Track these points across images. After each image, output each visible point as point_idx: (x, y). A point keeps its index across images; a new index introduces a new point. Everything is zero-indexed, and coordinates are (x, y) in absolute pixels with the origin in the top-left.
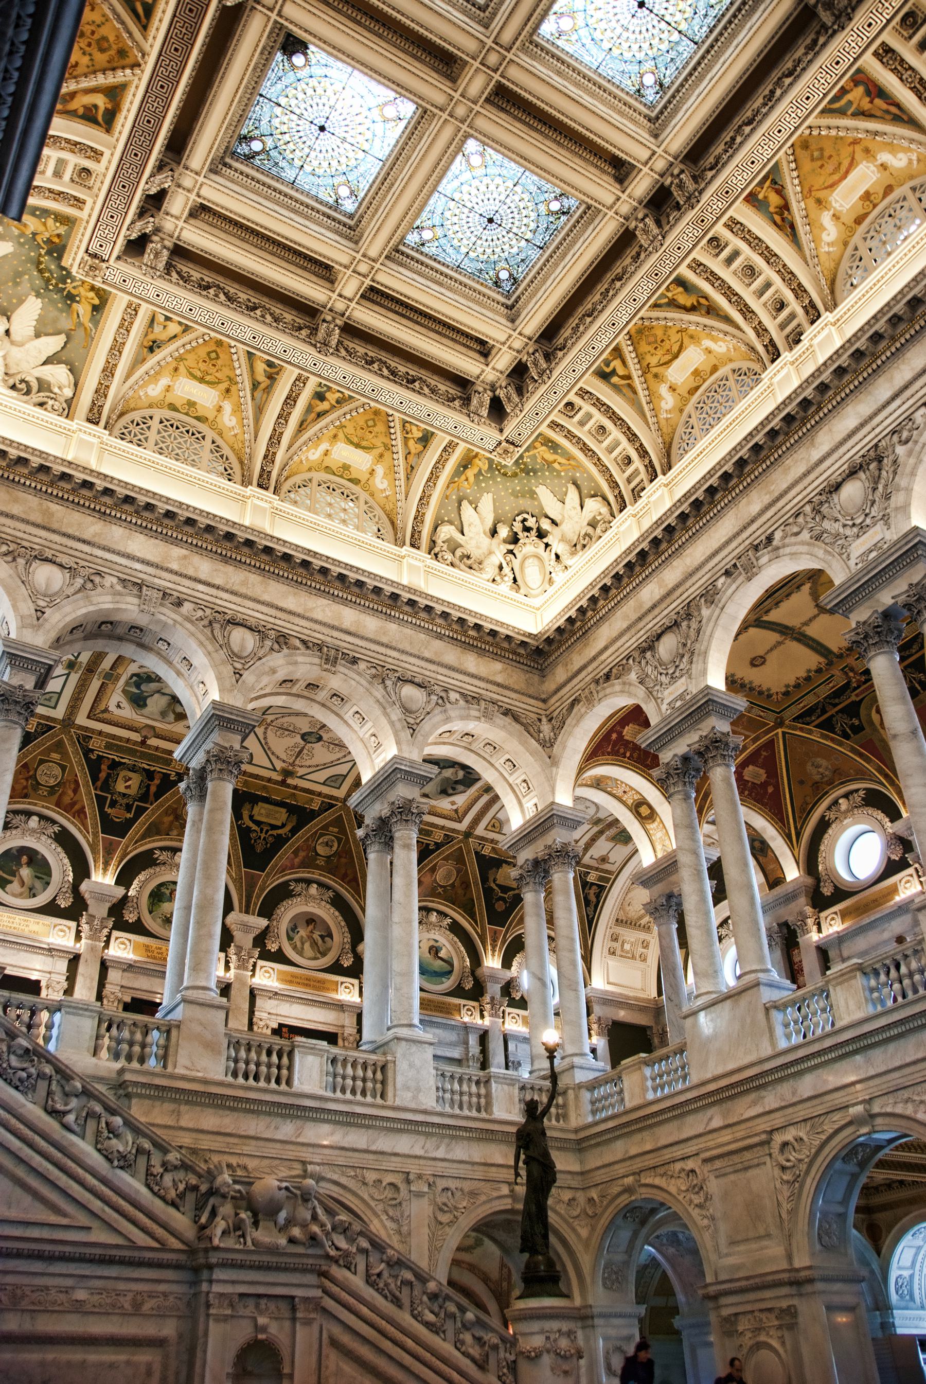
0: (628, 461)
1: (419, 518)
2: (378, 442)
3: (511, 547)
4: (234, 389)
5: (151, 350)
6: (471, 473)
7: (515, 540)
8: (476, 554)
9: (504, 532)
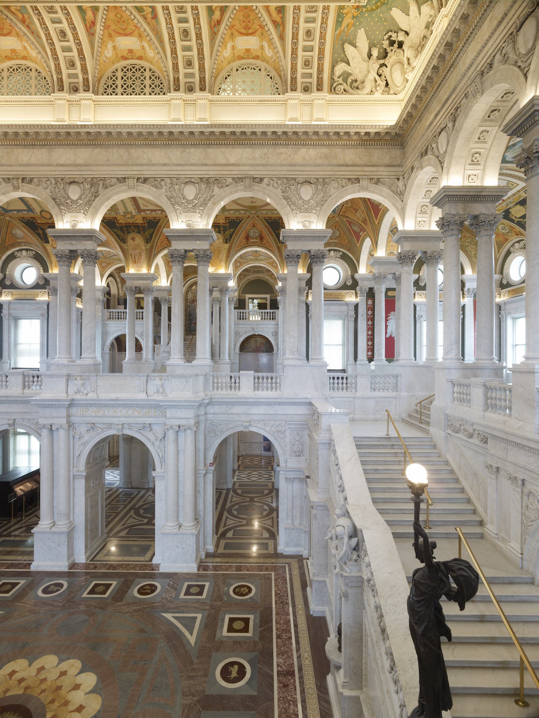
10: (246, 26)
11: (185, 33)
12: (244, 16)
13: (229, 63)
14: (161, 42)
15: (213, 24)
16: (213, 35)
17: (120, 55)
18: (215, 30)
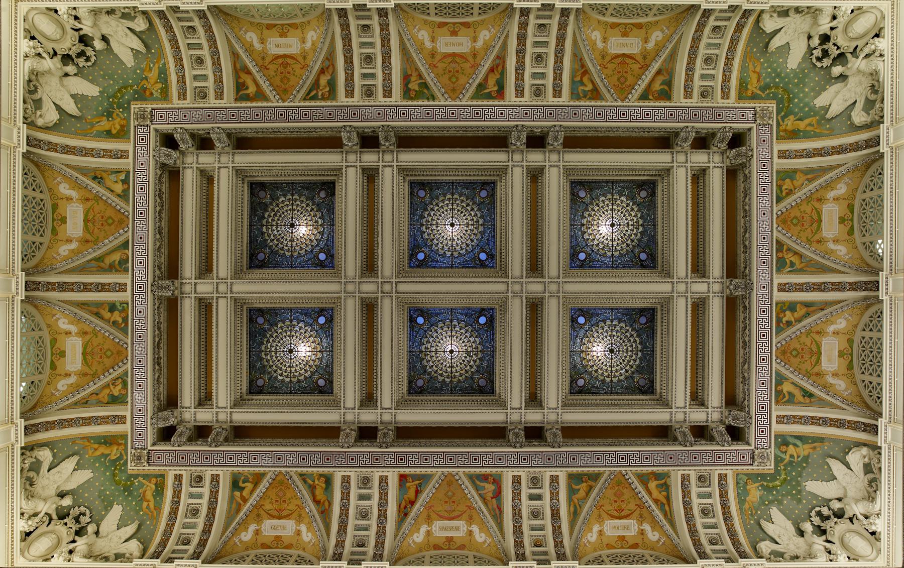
0: (716, 29)
1: (855, 147)
2: (808, 209)
3: (849, 56)
4: (814, 330)
5: (811, 395)
6: (802, 125)
7: (841, 58)
8: (867, 82)
9: (837, 70)
10: (285, 68)
11: (368, 59)
12: (289, 80)
13: (309, 22)
14: (404, 50)
15: (330, 70)
16: (330, 57)
17: (471, 30)
18: (327, 63)
